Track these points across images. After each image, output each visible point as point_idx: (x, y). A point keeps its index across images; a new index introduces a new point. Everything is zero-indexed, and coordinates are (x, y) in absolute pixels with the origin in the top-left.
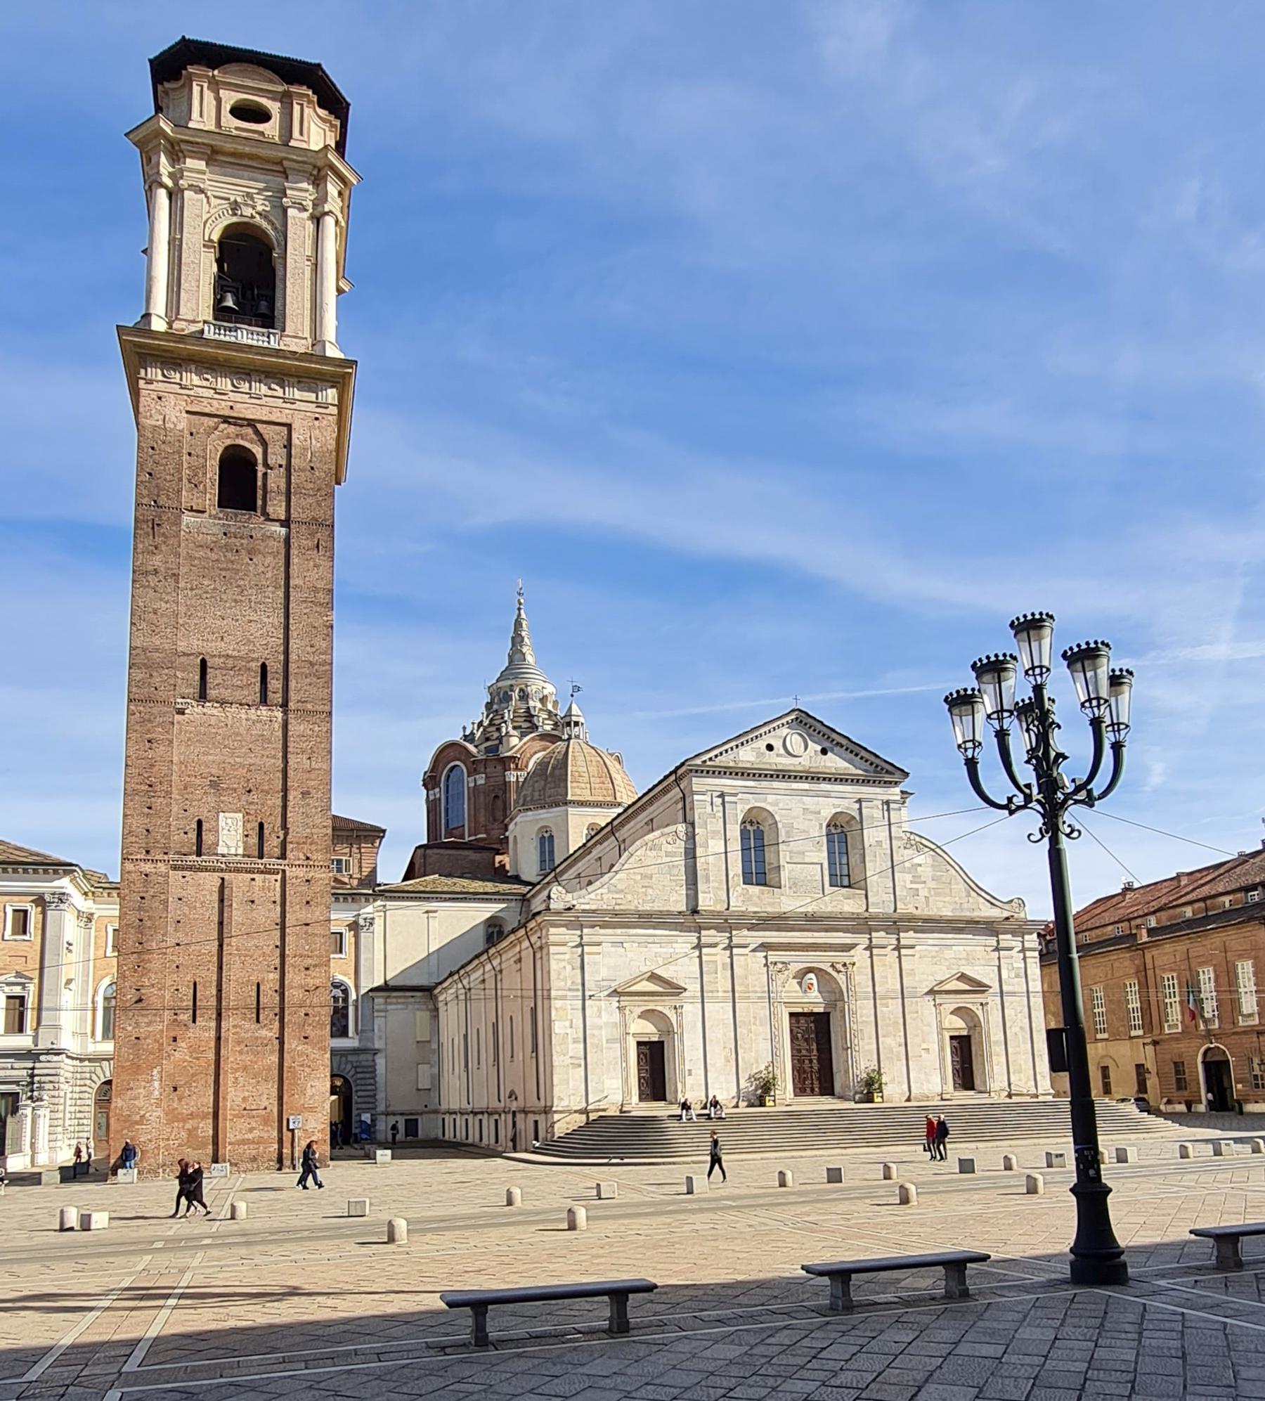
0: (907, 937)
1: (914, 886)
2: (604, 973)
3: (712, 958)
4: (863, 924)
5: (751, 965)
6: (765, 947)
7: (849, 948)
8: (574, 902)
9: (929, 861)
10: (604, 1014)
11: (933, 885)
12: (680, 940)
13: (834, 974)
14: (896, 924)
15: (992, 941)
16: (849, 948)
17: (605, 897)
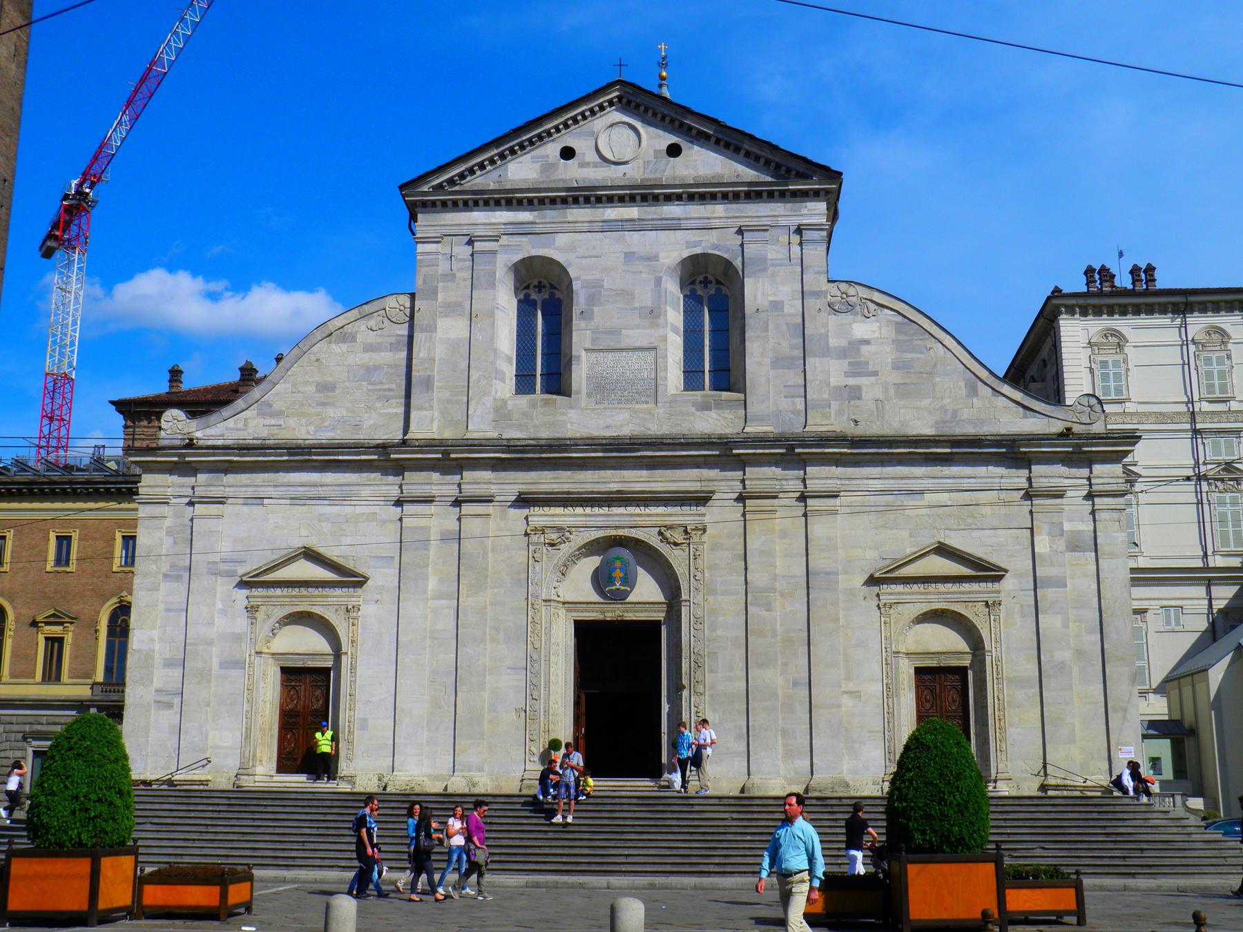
0: (821, 477)
1: (852, 381)
2: (225, 547)
3: (422, 522)
4: (726, 453)
5: (498, 528)
6: (524, 501)
7: (701, 499)
8: (198, 434)
9: (889, 333)
10: (221, 613)
11: (896, 377)
12: (365, 492)
13: (664, 549)
14: (794, 451)
15: (1018, 478)
16: (701, 499)
17: (252, 424)
